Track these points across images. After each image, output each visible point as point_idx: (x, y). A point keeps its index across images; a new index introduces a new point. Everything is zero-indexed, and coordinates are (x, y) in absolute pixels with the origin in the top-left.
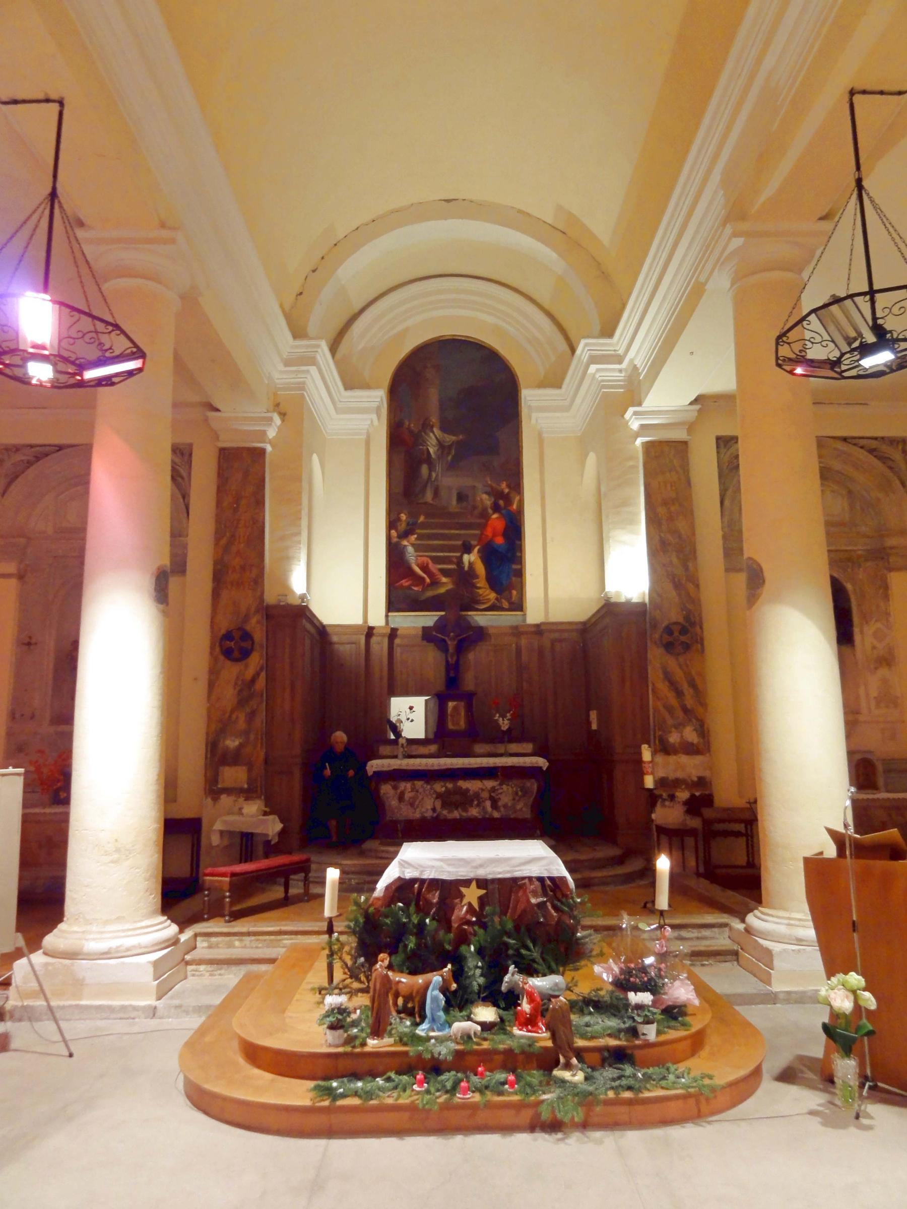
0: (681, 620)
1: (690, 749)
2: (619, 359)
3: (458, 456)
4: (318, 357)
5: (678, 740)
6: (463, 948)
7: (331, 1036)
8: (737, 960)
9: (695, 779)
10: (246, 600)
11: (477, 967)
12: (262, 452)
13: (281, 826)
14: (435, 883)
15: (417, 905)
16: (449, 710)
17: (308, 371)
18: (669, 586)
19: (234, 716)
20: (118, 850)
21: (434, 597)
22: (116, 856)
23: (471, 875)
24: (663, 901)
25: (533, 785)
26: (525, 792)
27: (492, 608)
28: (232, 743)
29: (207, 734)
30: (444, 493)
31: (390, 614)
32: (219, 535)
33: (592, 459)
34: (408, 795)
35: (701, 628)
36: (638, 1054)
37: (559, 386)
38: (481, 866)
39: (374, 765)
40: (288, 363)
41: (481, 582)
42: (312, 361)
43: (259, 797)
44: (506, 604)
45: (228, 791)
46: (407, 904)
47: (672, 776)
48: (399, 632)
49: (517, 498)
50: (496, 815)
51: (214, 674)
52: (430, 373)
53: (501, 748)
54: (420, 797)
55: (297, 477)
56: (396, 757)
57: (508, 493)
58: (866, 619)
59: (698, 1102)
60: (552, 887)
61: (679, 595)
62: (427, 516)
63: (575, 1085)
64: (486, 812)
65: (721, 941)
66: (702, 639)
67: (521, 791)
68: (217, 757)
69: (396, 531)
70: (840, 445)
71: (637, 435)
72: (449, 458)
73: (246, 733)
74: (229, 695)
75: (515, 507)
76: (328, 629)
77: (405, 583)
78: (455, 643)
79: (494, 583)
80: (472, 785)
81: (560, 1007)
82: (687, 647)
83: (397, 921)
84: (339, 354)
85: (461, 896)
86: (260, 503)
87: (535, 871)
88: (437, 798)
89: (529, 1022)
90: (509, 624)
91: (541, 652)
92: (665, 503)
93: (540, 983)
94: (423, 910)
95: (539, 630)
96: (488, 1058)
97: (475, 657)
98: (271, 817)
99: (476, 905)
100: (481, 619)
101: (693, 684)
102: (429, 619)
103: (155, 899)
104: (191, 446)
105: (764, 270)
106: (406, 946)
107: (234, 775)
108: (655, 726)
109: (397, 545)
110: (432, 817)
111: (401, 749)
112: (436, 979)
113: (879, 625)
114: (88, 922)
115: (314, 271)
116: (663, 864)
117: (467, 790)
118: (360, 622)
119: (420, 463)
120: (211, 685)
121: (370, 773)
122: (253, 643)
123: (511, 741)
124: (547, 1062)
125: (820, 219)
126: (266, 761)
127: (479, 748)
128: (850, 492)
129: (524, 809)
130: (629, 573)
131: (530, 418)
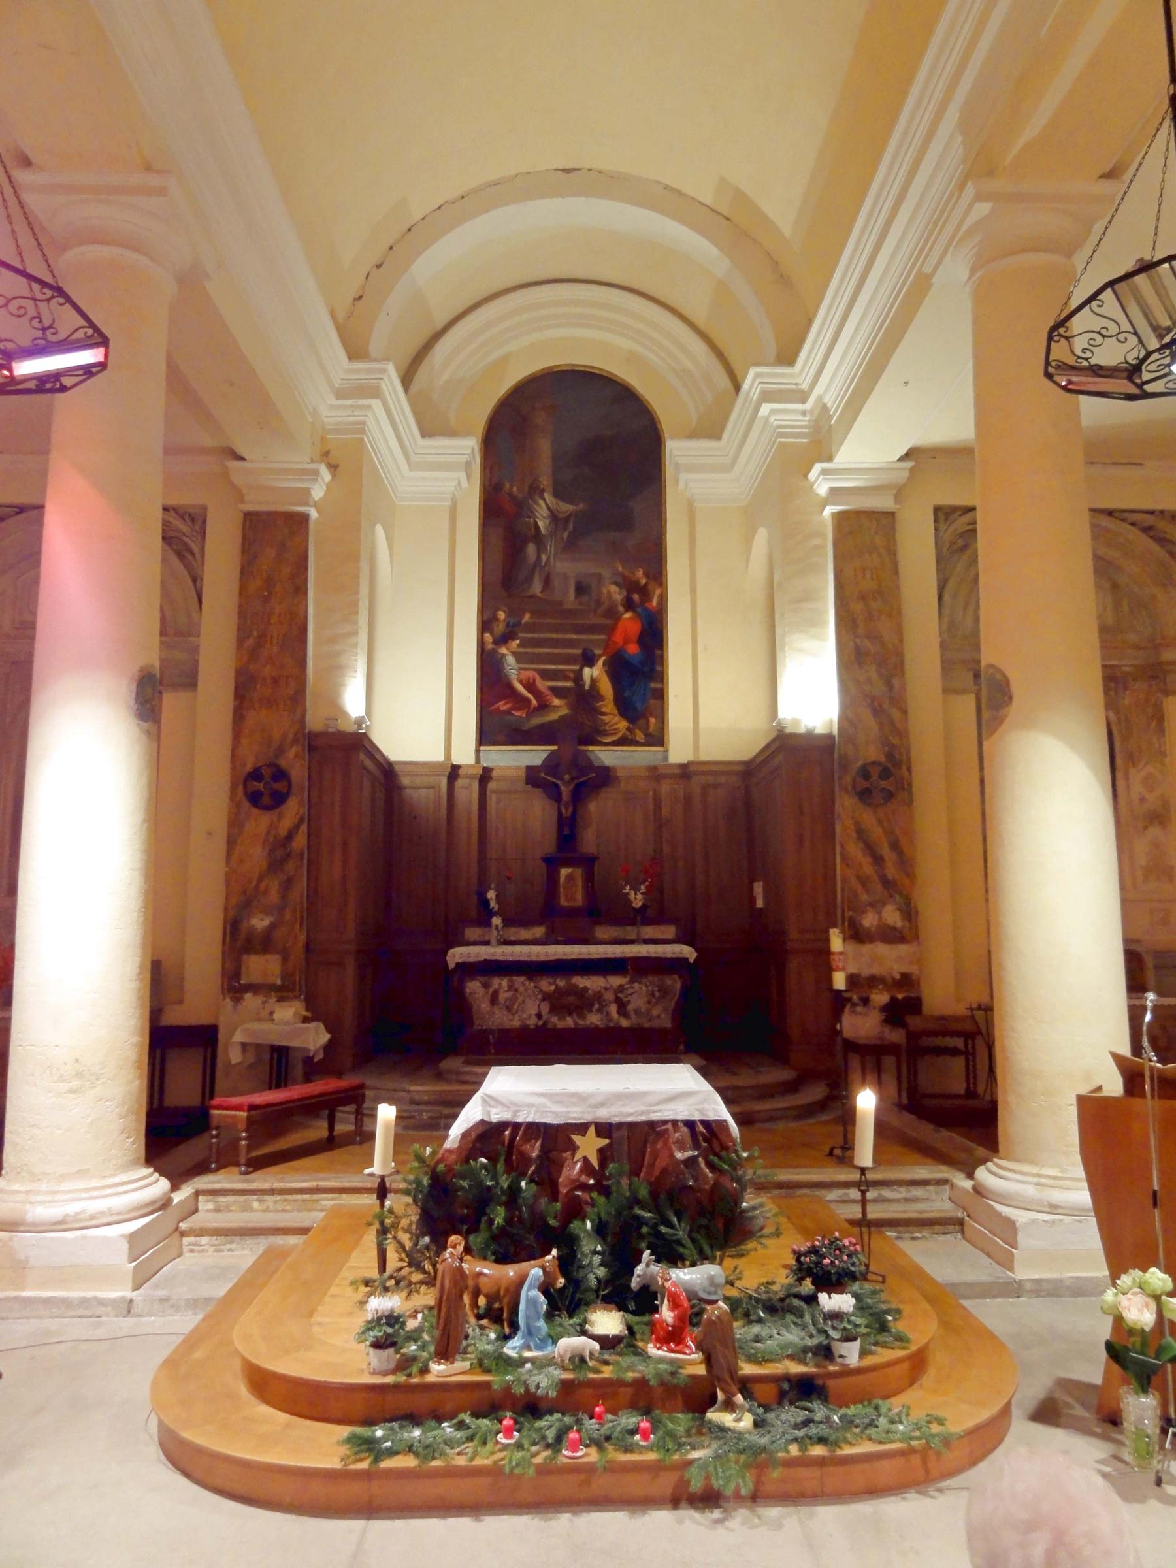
0: (882, 759)
1: (892, 936)
2: (802, 397)
3: (576, 533)
4: (383, 385)
5: (876, 923)
6: (575, 1225)
7: (376, 1358)
8: (962, 1232)
9: (898, 977)
10: (279, 724)
11: (595, 1252)
12: (303, 519)
13: (327, 1037)
14: (535, 1129)
15: (508, 1161)
16: (562, 879)
17: (369, 407)
18: (867, 716)
19: (263, 885)
20: (79, 1075)
21: (542, 726)
22: (76, 1083)
23: (587, 1117)
24: (865, 1153)
25: (675, 983)
26: (664, 991)
27: (623, 742)
28: (260, 922)
29: (226, 910)
30: (556, 582)
31: (482, 748)
32: (242, 634)
33: (762, 536)
34: (503, 996)
35: (909, 770)
36: (831, 1384)
37: (717, 436)
38: (602, 1104)
39: (457, 955)
40: (340, 394)
41: (608, 705)
42: (374, 392)
43: (296, 997)
44: (640, 737)
45: (254, 988)
46: (493, 1159)
47: (866, 972)
48: (494, 774)
49: (658, 592)
50: (625, 1023)
51: (235, 826)
52: (540, 418)
53: (631, 932)
54: (520, 999)
55: (352, 557)
56: (487, 943)
57: (646, 584)
59: (924, 1461)
60: (707, 1134)
61: (881, 724)
62: (533, 613)
63: (739, 1436)
64: (610, 1020)
65: (938, 1204)
66: (910, 785)
67: (659, 991)
68: (238, 941)
69: (492, 634)
71: (825, 503)
72: (565, 535)
73: (281, 909)
74: (256, 856)
75: (655, 603)
76: (397, 768)
77: (503, 706)
78: (571, 787)
79: (625, 707)
80: (590, 983)
81: (718, 1317)
82: (890, 796)
83: (480, 1183)
84: (414, 389)
85: (574, 1148)
86: (301, 590)
87: (681, 1111)
88: (544, 999)
89: (672, 1337)
90: (645, 763)
91: (688, 799)
92: (863, 598)
93: (685, 1276)
94: (516, 1167)
95: (685, 772)
96: (608, 1391)
97: (600, 809)
98: (312, 1025)
99: (595, 1162)
100: (605, 756)
101: (895, 846)
102: (535, 755)
103: (135, 1143)
104: (204, 509)
105: (1023, 251)
106: (491, 1222)
107: (262, 967)
108: (843, 903)
109: (494, 651)
110: (537, 1026)
111: (495, 933)
112: (535, 1272)
114: (34, 1178)
115: (379, 266)
116: (866, 1101)
117: (585, 989)
118: (438, 756)
119: (525, 542)
120: (231, 843)
121: (451, 966)
122: (290, 786)
123: (648, 922)
124: (699, 1398)
125: (1101, 177)
126: (307, 947)
127: (601, 932)
129: (663, 1016)
130: (811, 694)
131: (677, 481)
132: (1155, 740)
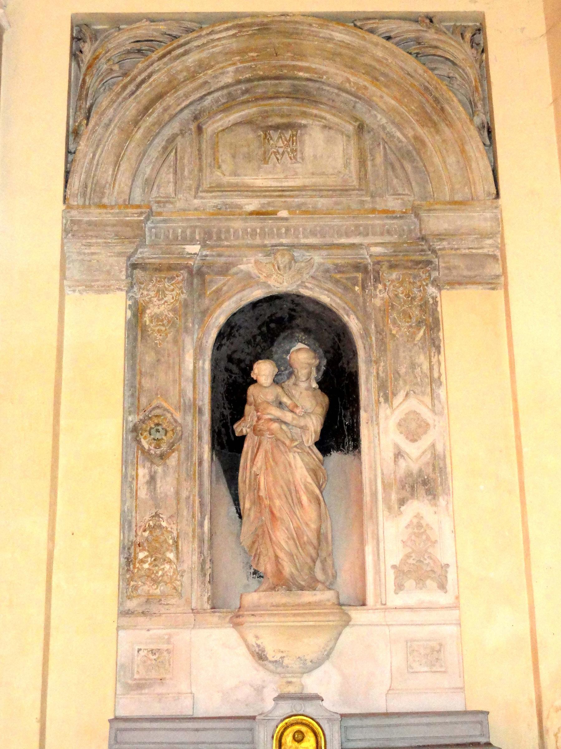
58: (386, 392)
70: (340, 35)
113: (413, 404)
128: (361, 128)
132: (422, 359)
